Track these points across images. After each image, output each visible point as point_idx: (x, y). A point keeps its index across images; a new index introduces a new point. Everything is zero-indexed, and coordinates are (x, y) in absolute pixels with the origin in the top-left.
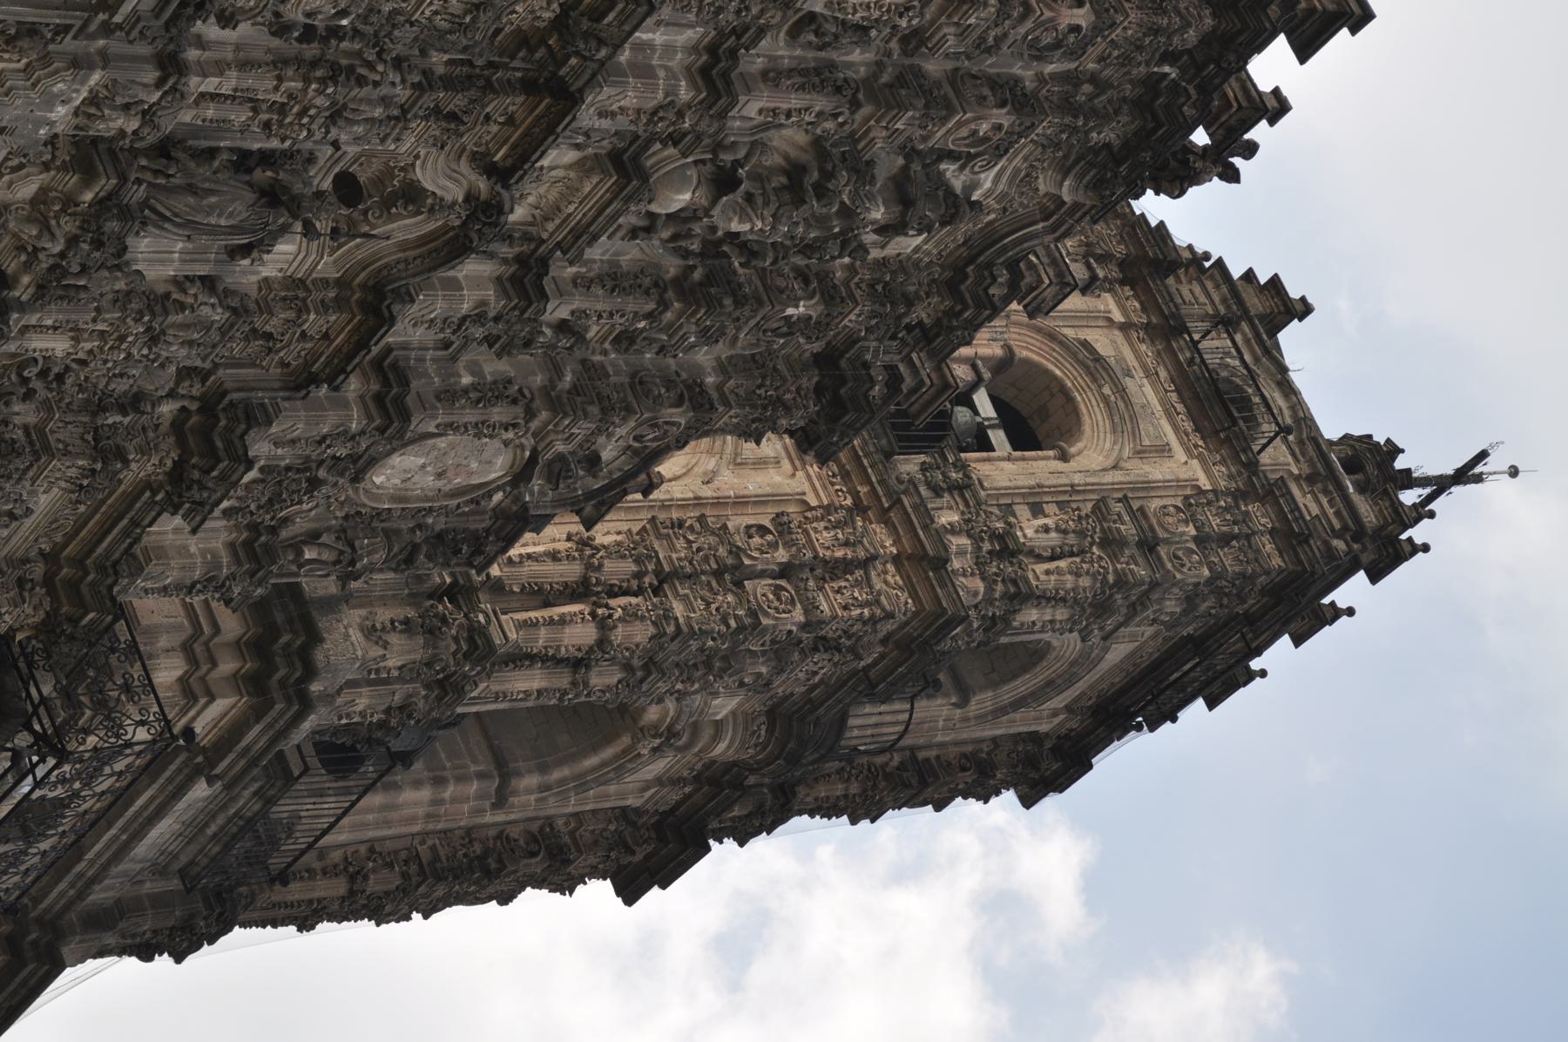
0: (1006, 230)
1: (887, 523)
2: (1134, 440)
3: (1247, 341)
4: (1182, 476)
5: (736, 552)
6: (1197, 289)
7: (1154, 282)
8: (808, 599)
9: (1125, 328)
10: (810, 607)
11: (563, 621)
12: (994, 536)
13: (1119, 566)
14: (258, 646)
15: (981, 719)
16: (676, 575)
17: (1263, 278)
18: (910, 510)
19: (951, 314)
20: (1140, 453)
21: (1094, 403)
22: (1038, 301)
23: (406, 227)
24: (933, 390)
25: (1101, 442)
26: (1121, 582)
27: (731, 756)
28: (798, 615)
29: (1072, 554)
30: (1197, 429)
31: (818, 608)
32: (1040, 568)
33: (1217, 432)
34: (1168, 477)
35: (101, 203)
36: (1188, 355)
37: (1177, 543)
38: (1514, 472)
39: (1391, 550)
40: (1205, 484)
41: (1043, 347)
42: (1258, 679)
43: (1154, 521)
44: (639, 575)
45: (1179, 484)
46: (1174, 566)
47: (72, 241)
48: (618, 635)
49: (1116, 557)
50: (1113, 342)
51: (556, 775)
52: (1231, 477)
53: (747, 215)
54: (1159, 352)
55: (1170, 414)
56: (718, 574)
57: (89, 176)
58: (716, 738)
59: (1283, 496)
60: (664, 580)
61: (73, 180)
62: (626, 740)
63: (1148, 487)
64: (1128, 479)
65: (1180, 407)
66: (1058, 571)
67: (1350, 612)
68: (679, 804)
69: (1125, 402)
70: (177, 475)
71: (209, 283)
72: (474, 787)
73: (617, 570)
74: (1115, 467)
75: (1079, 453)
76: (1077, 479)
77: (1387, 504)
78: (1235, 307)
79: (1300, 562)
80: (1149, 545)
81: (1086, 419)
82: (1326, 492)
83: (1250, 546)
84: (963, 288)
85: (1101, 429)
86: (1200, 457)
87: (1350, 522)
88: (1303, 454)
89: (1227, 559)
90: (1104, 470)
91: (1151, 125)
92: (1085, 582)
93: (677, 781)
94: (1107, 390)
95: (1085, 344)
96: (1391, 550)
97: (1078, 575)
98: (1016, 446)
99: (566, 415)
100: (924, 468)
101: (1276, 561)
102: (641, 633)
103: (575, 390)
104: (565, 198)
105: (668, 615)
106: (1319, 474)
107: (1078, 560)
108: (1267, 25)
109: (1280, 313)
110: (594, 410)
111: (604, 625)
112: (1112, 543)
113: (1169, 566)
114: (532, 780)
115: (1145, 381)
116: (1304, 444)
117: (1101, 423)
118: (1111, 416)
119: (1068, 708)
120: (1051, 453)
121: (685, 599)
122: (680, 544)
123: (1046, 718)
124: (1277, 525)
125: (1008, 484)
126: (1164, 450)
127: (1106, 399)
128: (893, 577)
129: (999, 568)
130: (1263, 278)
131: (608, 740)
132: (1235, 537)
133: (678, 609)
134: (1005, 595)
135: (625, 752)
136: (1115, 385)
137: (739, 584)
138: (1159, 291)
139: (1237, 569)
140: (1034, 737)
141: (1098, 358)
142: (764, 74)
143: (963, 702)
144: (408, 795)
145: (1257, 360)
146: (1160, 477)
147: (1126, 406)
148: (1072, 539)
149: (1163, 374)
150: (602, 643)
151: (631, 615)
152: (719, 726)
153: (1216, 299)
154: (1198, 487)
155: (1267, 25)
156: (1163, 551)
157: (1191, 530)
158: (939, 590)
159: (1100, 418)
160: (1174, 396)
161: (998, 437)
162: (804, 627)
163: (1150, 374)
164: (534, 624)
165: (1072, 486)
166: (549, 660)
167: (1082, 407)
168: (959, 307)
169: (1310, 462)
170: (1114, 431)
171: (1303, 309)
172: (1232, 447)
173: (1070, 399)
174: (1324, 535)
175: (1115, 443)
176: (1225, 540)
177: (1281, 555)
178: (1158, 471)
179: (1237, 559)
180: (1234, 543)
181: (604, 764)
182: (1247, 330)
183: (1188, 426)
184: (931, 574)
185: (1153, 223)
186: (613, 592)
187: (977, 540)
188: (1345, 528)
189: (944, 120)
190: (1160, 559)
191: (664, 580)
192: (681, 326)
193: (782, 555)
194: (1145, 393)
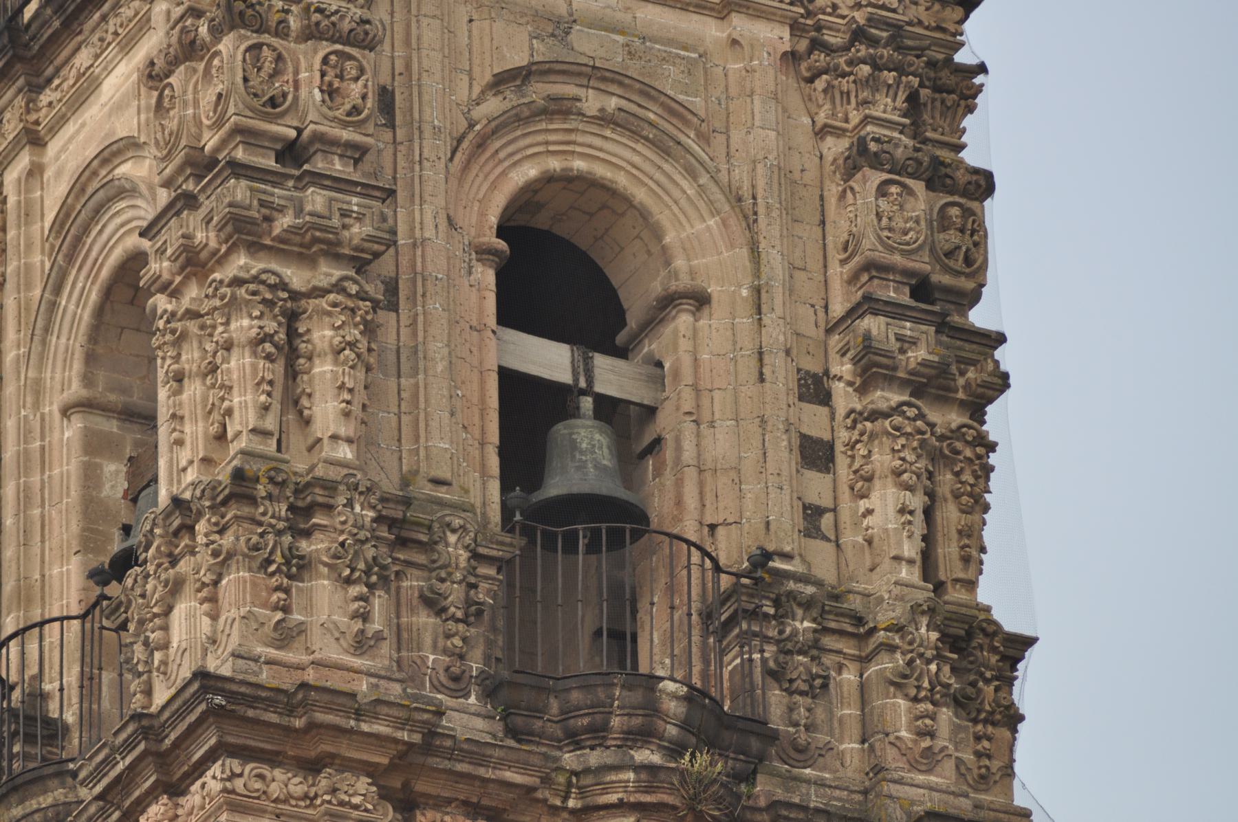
2: (686, 122)
13: (961, 395)
21: (597, 142)
25: (677, 194)
41: (487, 169)
43: (897, 259)
46: (968, 276)
49: (948, 389)
69: (612, 81)
81: (622, 181)
85: (647, 167)
94: (592, 102)
117: (636, 159)
118: (636, 134)
127: (604, 119)
136: (580, 74)
147: (621, 84)
159: (627, 154)
167: (601, 171)
170: (666, 152)
175: (692, 174)
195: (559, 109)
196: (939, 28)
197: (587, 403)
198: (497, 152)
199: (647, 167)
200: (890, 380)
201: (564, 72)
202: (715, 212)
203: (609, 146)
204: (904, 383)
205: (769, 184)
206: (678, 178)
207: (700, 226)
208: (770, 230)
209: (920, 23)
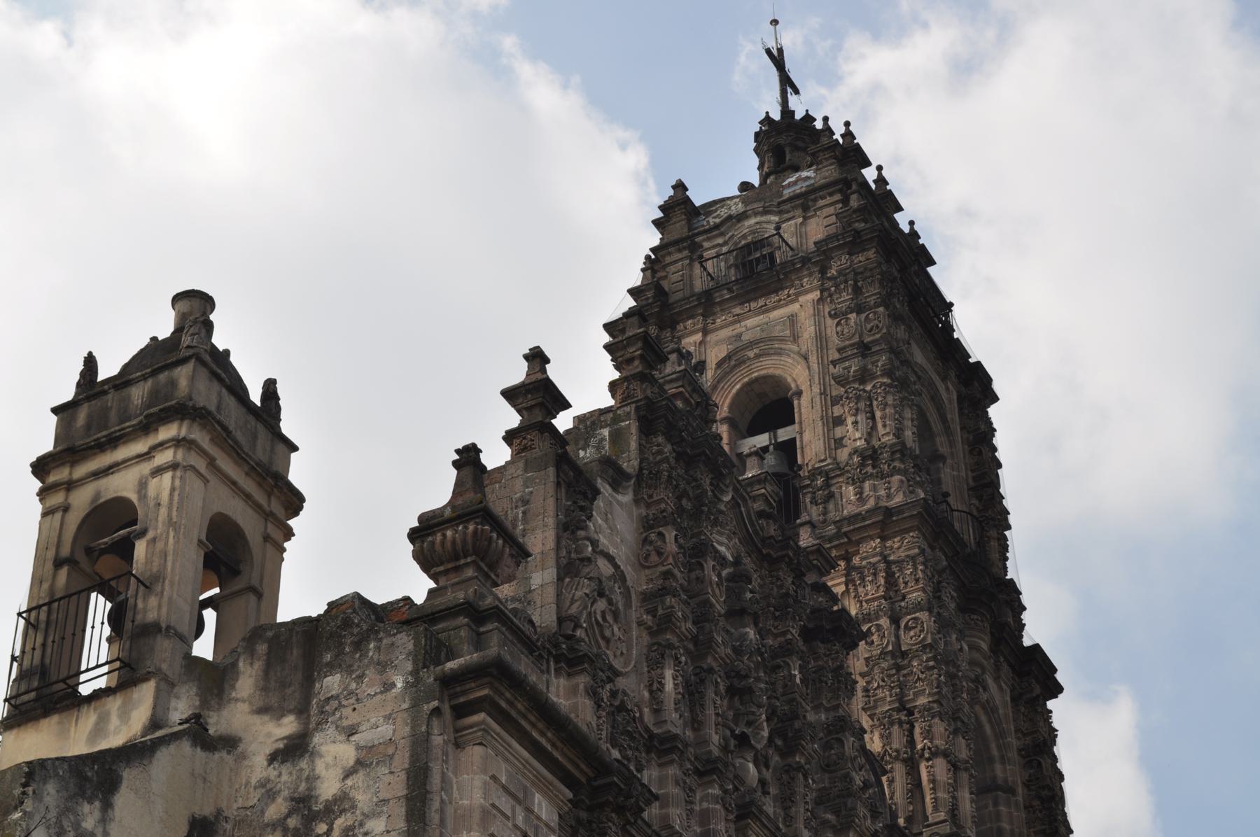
0: (744, 531)
1: (858, 542)
2: (786, 341)
3: (709, 239)
4: (812, 312)
5: (883, 653)
6: (672, 268)
7: (675, 308)
8: (913, 608)
9: (705, 332)
10: (918, 607)
11: (933, 781)
12: (862, 465)
13: (879, 373)
15: (952, 444)
16: (901, 699)
17: (659, 214)
18: (852, 527)
20: (795, 338)
21: (760, 364)
22: (772, 494)
24: (820, 559)
25: (788, 365)
26: (888, 373)
27: (987, 638)
28: (923, 615)
29: (871, 405)
30: (776, 291)
31: (919, 602)
32: (881, 430)
33: (780, 279)
34: (813, 323)
36: (725, 292)
37: (862, 327)
38: (775, 22)
39: (852, 154)
40: (816, 295)
41: (721, 395)
42: (851, 128)
43: (847, 343)
44: (901, 723)
45: (817, 314)
48: (939, 742)
49: (871, 374)
50: (717, 343)
51: (995, 752)
52: (810, 275)
53: (759, 725)
54: (722, 310)
55: (765, 310)
56: (899, 668)
59: (827, 244)
60: (903, 706)
63: (821, 340)
64: (815, 352)
65: (761, 302)
66: (884, 417)
67: (847, 124)
68: (1010, 665)
70: (620, 810)
72: (1003, 809)
73: (898, 740)
74: (806, 358)
75: (795, 380)
76: (816, 390)
77: (821, 154)
78: (685, 244)
79: (872, 238)
80: (864, 349)
81: (771, 371)
82: (815, 200)
83: (862, 273)
84: (775, 556)
85: (778, 362)
86: (798, 295)
87: (837, 187)
88: (788, 212)
89: (872, 293)
90: (809, 368)
91: (703, 458)
92: (890, 399)
93: (997, 668)
94: (751, 354)
95: (719, 365)
96: (852, 154)
97: (886, 405)
98: (791, 421)
99: (854, 821)
100: (814, 502)
101: (871, 254)
102: (939, 727)
103: (837, 813)
105: (927, 708)
106: (803, 204)
107: (875, 403)
108: (664, 403)
109: (685, 208)
110: (850, 801)
111: (934, 755)
112: (864, 376)
113: (878, 336)
114: (998, 768)
115: (743, 324)
116: (782, 211)
117: (773, 362)
118: (769, 355)
119: (944, 379)
120: (796, 402)
121: (917, 695)
122: (880, 693)
123: (948, 393)
124: (846, 250)
125: (822, 441)
126: (792, 319)
127: (757, 356)
128: (894, 543)
129: (885, 463)
130: (659, 214)
132: (856, 282)
133: (922, 701)
134: (902, 461)
136: (747, 347)
137: (904, 655)
138: (681, 306)
139: (877, 285)
140: (961, 399)
141: (729, 357)
142: (694, 730)
143: (942, 458)
145: (722, 234)
146: (813, 328)
147: (762, 342)
148: (862, 405)
149: (737, 310)
150: (945, 754)
151: (928, 734)
153: (679, 256)
154: (818, 300)
155: (664, 403)
156: (867, 339)
157: (853, 316)
158: (905, 515)
159: (770, 362)
160: (753, 305)
161: (784, 434)
162: (930, 610)
163: (739, 319)
164: (936, 800)
165: (821, 394)
166: (955, 786)
167: (762, 373)
168: (787, 559)
169: (794, 208)
170: (780, 354)
171: (680, 187)
172: (790, 272)
173: (757, 379)
174: (849, 212)
175: (789, 355)
176: (857, 290)
177: (868, 250)
178: (808, 330)
179: (870, 284)
180: (859, 284)
181: (990, 721)
182: (701, 238)
183: (774, 298)
184: (894, 518)
185: (631, 303)
186: (911, 742)
187: (867, 477)
188: (840, 191)
189: (712, 605)
190: (872, 342)
191: (903, 706)
192: (809, 754)
193: (884, 622)
194: (752, 325)
195: (741, 362)
196: (868, 260)
197: (771, 448)
198: (723, 387)
199: (778, 362)
200: (849, 383)
201: (742, 350)
202: (798, 363)
203: (763, 363)
204: (854, 381)
205: (812, 344)
206: (787, 360)
207: (797, 370)
208: (813, 359)
209: (861, 262)
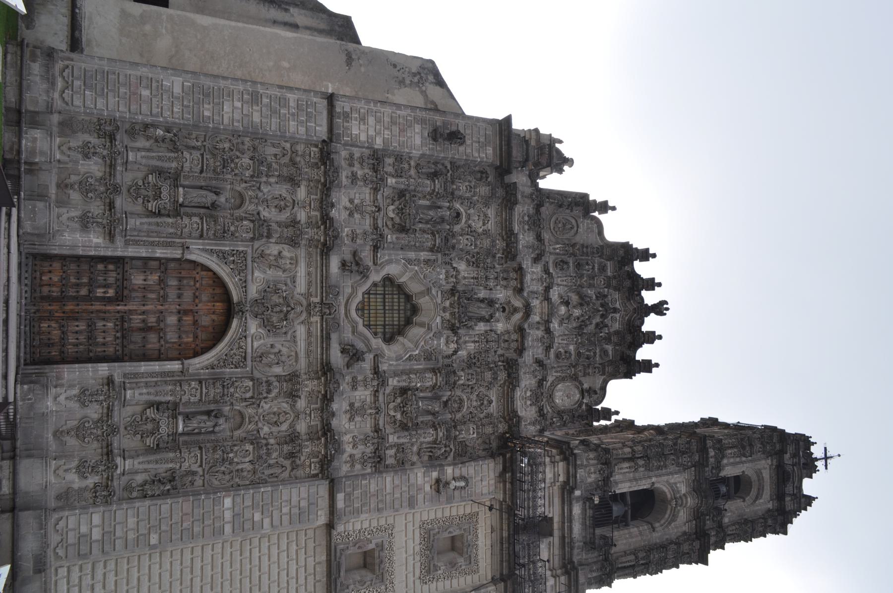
14: (562, 453)
19: (634, 336)
23: (518, 316)
35: (459, 299)
38: (839, 455)
47: (459, 308)
57: (454, 296)
58: (686, 498)
61: (453, 298)
62: (669, 507)
71: (491, 330)
93: (690, 521)
104: (542, 310)
131: (666, 509)
135: (671, 510)
144: (632, 530)
152: (684, 495)
